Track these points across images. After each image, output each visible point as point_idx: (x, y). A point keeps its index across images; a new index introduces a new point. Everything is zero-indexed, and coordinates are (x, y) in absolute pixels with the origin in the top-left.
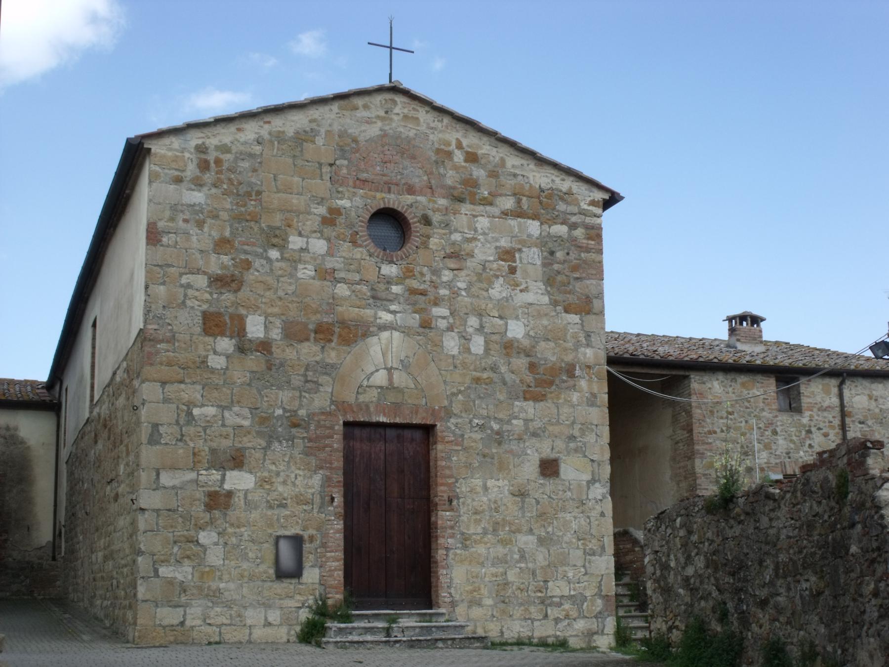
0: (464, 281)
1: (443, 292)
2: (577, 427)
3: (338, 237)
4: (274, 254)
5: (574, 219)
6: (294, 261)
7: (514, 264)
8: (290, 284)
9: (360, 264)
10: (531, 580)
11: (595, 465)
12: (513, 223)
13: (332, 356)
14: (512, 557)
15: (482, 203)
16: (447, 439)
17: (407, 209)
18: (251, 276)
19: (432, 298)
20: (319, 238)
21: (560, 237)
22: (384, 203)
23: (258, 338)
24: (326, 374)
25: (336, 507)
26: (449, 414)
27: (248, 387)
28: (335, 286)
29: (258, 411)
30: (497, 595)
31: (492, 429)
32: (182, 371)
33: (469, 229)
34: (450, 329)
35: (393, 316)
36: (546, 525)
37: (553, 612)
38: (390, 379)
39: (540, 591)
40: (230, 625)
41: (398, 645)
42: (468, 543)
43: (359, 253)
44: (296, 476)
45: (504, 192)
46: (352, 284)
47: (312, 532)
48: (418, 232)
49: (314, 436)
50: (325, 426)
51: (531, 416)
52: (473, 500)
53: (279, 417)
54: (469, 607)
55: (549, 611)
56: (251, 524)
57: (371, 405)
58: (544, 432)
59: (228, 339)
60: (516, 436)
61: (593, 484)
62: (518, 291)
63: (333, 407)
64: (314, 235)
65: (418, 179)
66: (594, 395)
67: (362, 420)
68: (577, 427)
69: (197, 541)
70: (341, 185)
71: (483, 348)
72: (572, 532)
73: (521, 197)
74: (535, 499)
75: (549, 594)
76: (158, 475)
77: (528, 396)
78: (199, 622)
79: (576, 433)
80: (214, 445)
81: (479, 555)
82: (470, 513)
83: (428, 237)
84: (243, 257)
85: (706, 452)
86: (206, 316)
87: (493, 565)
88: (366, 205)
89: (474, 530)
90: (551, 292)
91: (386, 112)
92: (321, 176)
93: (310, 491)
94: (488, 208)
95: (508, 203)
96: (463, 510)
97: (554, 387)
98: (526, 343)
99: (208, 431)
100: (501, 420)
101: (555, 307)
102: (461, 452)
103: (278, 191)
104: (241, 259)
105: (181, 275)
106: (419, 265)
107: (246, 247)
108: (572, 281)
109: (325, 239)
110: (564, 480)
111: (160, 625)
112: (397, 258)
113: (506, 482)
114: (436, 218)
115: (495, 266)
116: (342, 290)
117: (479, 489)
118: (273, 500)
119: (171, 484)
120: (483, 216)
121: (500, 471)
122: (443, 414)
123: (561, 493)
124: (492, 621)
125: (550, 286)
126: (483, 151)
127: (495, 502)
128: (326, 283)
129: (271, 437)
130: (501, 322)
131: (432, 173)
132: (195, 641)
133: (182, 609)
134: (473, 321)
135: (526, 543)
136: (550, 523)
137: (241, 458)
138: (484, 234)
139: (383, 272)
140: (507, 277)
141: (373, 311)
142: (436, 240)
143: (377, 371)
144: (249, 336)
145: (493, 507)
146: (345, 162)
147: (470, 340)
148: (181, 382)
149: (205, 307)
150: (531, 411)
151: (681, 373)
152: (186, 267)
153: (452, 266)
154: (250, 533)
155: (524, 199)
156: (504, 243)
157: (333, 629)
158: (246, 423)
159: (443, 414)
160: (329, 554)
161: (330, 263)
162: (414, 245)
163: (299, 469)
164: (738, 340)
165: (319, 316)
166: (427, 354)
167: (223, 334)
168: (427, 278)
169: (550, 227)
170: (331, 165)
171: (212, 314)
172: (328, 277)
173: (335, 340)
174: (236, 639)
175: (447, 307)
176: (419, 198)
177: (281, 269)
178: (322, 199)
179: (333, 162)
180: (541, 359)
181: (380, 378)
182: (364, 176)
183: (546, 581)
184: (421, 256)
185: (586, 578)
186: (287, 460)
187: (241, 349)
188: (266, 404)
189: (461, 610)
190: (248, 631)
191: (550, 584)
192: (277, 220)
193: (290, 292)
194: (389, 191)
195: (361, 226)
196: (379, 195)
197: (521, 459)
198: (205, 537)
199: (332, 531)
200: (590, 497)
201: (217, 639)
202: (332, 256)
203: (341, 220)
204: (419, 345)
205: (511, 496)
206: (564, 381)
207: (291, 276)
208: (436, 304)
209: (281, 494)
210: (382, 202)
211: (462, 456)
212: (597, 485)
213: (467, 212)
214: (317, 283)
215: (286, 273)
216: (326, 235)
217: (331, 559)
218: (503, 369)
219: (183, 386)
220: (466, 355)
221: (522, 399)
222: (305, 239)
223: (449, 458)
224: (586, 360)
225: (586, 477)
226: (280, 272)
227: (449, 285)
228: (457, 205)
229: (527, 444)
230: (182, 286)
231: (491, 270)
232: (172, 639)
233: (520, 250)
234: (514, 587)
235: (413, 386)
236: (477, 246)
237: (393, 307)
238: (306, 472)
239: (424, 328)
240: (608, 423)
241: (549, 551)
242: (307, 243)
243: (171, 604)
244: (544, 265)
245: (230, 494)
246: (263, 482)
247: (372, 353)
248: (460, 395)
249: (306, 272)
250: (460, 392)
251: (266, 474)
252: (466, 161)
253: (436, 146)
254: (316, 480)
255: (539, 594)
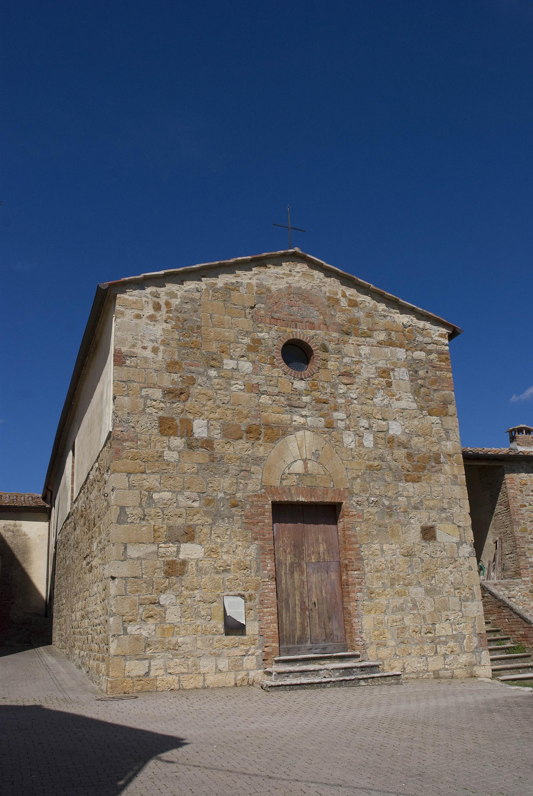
0: (355, 393)
1: (340, 401)
2: (446, 501)
3: (260, 360)
4: (213, 373)
5: (429, 347)
6: (228, 379)
7: (390, 380)
8: (226, 396)
9: (278, 380)
10: (423, 623)
11: (461, 529)
12: (387, 350)
13: (261, 451)
14: (407, 606)
15: (363, 335)
16: (351, 514)
17: (310, 340)
18: (195, 390)
19: (333, 405)
20: (246, 361)
21: (421, 360)
22: (293, 336)
23: (202, 438)
24: (257, 464)
25: (270, 571)
26: (352, 494)
27: (196, 476)
28: (260, 397)
29: (205, 495)
30: (398, 637)
31: (384, 505)
32: (144, 464)
33: (356, 355)
34: (348, 428)
35: (304, 419)
36: (430, 578)
37: (441, 649)
38: (306, 467)
39: (430, 633)
40: (187, 673)
41: (328, 685)
42: (373, 595)
43: (276, 372)
44: (236, 546)
45: (378, 328)
46: (273, 396)
47: (251, 592)
48: (319, 356)
49: (249, 514)
50: (258, 506)
51: (411, 494)
52: (374, 561)
53: (222, 499)
54: (377, 649)
55: (439, 650)
56: (203, 587)
57: (292, 488)
58: (422, 505)
59: (180, 438)
60: (402, 510)
61: (462, 545)
62: (394, 400)
63: (263, 490)
64: (242, 359)
65: (317, 317)
66: (455, 477)
67: (286, 500)
68: (446, 501)
69: (158, 603)
70: (260, 322)
71: (372, 443)
72: (450, 584)
73: (390, 331)
74: (420, 558)
75: (437, 635)
76: (125, 548)
77: (408, 478)
78: (161, 672)
79: (446, 506)
80: (171, 523)
81: (382, 605)
82: (373, 571)
83: (326, 360)
84: (189, 375)
85: (520, 520)
86: (162, 420)
87: (393, 613)
88: (279, 337)
89: (376, 585)
90: (418, 400)
91: (290, 271)
92: (246, 316)
93: (248, 558)
94: (368, 339)
95: (382, 336)
96: (367, 569)
97: (426, 471)
98: (404, 438)
99: (165, 512)
100: (390, 497)
101: (422, 411)
102: (363, 524)
103: (214, 326)
104: (187, 377)
105: (141, 388)
106: (321, 381)
107: (193, 368)
108: (432, 392)
109: (251, 362)
110: (440, 543)
111: (129, 676)
112: (305, 376)
113: (398, 546)
114: (331, 346)
115: (376, 382)
116: (264, 399)
117: (378, 552)
118: (220, 567)
119: (137, 556)
120: (365, 345)
121: (393, 537)
122: (347, 494)
123: (438, 553)
124: (396, 660)
125: (417, 395)
126: (361, 299)
127: (391, 562)
128: (253, 394)
129: (216, 515)
130: (384, 423)
131: (326, 314)
132: (159, 689)
133: (146, 662)
134: (364, 423)
135: (416, 594)
136: (433, 577)
137: (193, 533)
138: (367, 358)
139: (295, 386)
140: (386, 389)
141: (290, 416)
142: (333, 363)
143: (295, 461)
144: (196, 435)
145: (389, 565)
146: (263, 306)
147: (362, 436)
148: (144, 473)
149: (161, 413)
150: (411, 489)
151: (497, 464)
152: (144, 383)
153: (346, 381)
154: (202, 595)
155: (393, 333)
156: (381, 364)
157: (274, 673)
158: (196, 504)
159: (347, 494)
160: (265, 610)
161: (255, 380)
162: (316, 366)
163: (239, 541)
164: (518, 444)
165: (248, 420)
166: (332, 448)
167: (175, 435)
168: (328, 391)
169: (412, 353)
170: (252, 308)
171: (167, 419)
172: (254, 390)
173: (262, 439)
174: (192, 686)
175: (344, 412)
176: (318, 332)
177: (218, 384)
178: (247, 332)
179: (253, 305)
180: (415, 450)
181: (298, 467)
182: (276, 316)
183: (433, 624)
184: (322, 375)
185: (463, 620)
186: (228, 533)
187: (190, 446)
188: (211, 489)
189: (371, 651)
190: (202, 678)
191: (437, 626)
192: (214, 347)
193: (226, 402)
194: (296, 327)
195: (276, 352)
196: (288, 330)
197: (406, 527)
198: (164, 599)
199: (267, 591)
200: (460, 555)
201: (177, 686)
202: (257, 374)
203: (261, 348)
204: (326, 441)
205: (402, 557)
206: (433, 467)
207: (226, 389)
208: (336, 410)
209: (225, 562)
210: (291, 335)
211: (364, 526)
212: (464, 545)
213: (353, 342)
214: (247, 395)
215: (222, 387)
216: (251, 359)
217: (268, 614)
218: (389, 458)
219: (144, 476)
220: (361, 448)
221: (404, 481)
222: (236, 362)
223: (354, 528)
224: (448, 450)
225: (456, 539)
226: (218, 387)
227: (344, 395)
228: (346, 338)
229: (410, 516)
230: (142, 397)
231: (373, 384)
232: (139, 688)
233: (393, 370)
234: (411, 630)
235: (323, 473)
236: (362, 367)
237: (304, 413)
238: (244, 542)
239: (328, 428)
240: (467, 498)
241: (434, 600)
242: (237, 364)
243: (137, 657)
244: (412, 381)
245: (184, 563)
246: (211, 552)
247: (291, 448)
248: (358, 479)
249: (237, 386)
250: (358, 476)
251: (214, 546)
252: (349, 306)
253: (328, 294)
254: (253, 549)
255: (429, 635)
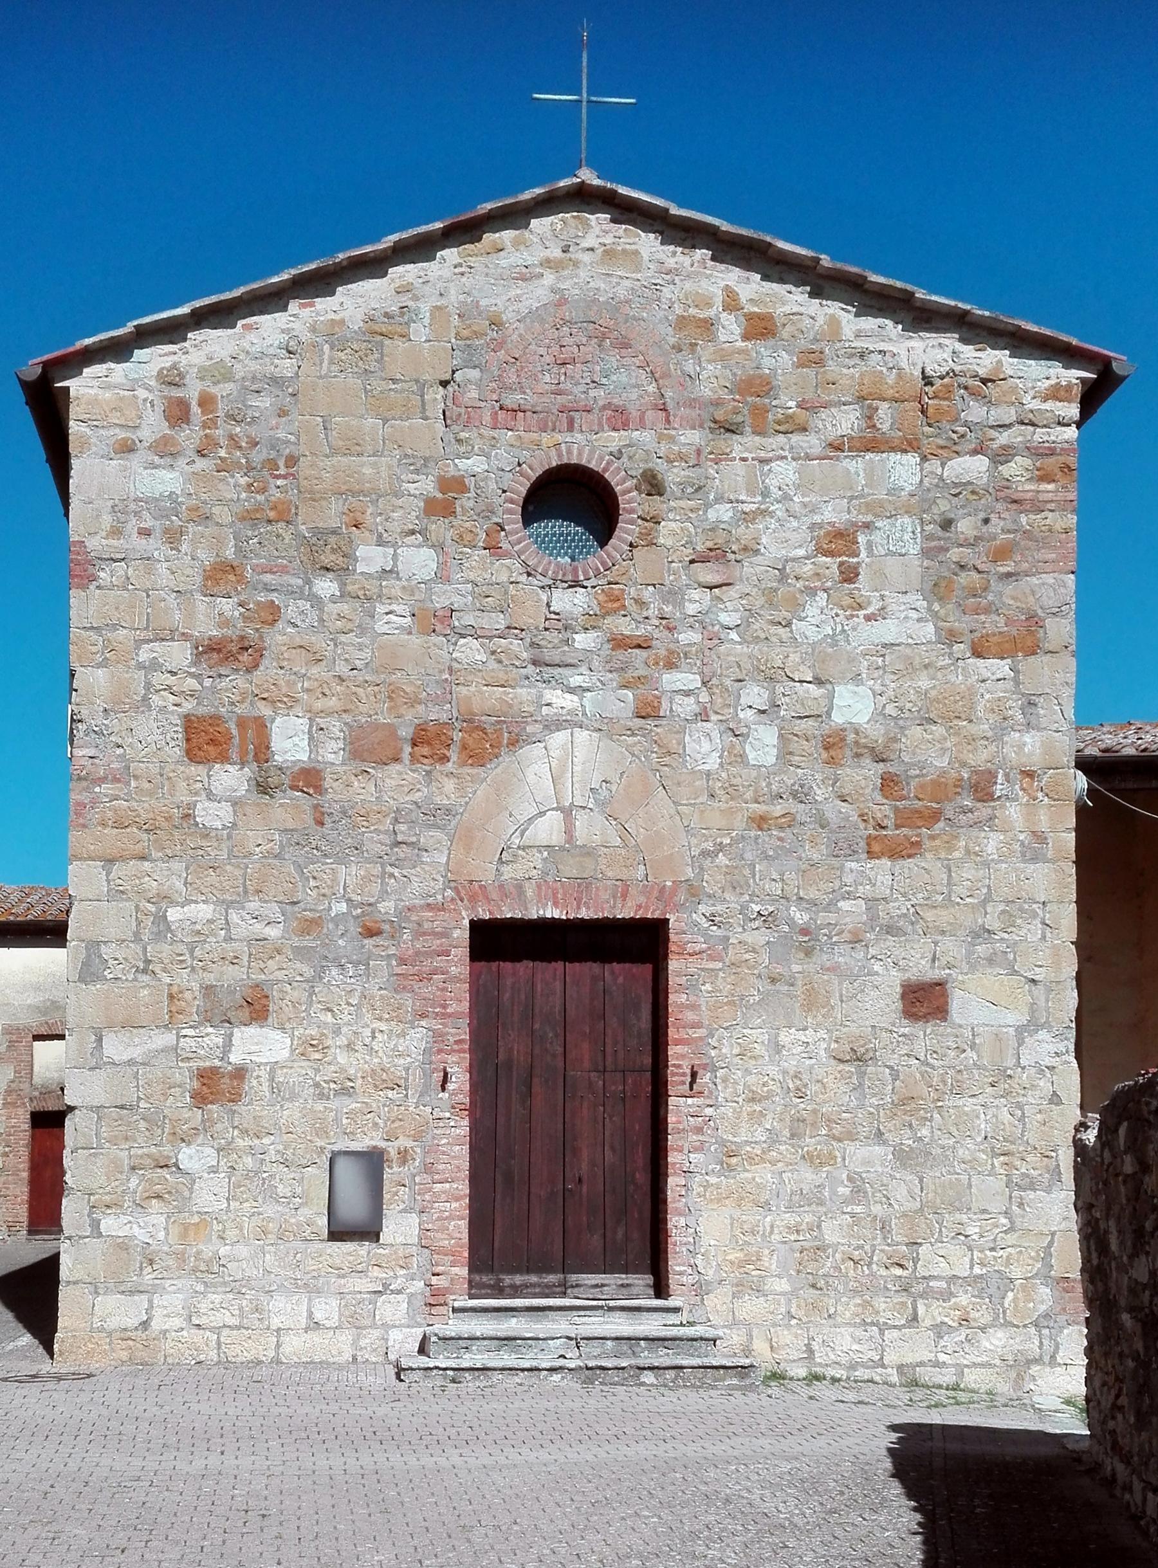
1: (688, 637)
4: (326, 587)
5: (1003, 438)
12: (855, 466)
14: (834, 1192)
16: (690, 948)
18: (277, 638)
19: (663, 652)
20: (419, 546)
21: (970, 483)
22: (560, 455)
24: (435, 826)
25: (453, 1094)
26: (695, 893)
28: (456, 644)
30: (799, 1272)
31: (791, 922)
32: (145, 836)
33: (751, 492)
34: (703, 716)
35: (575, 698)
37: (931, 1312)
38: (569, 832)
40: (238, 1328)
42: (734, 1160)
43: (505, 570)
44: (373, 1032)
46: (490, 638)
47: (404, 1142)
48: (632, 511)
52: (747, 1072)
53: (338, 919)
55: (921, 1310)
57: (527, 884)
59: (237, 767)
60: (846, 936)
63: (449, 893)
66: (1039, 837)
69: (176, 1165)
72: (979, 1139)
75: (922, 1271)
76: (100, 1040)
77: (876, 848)
80: (210, 978)
86: (191, 725)
87: (790, 1208)
90: (942, 612)
93: (402, 1061)
94: (795, 438)
97: (941, 824)
98: (876, 733)
99: (197, 952)
103: (334, 451)
104: (258, 603)
105: (139, 643)
106: (635, 583)
109: (433, 546)
110: (961, 1026)
111: (101, 1329)
112: (585, 573)
113: (822, 1034)
114: (673, 476)
115: (807, 568)
116: (471, 651)
119: (125, 1058)
121: (810, 1010)
122: (682, 897)
126: (787, 309)
127: (797, 1076)
128: (434, 639)
131: (667, 375)
133: (145, 1297)
134: (755, 695)
135: (867, 1162)
137: (264, 1001)
142: (673, 525)
143: (542, 814)
146: (474, 374)
147: (746, 736)
148: (143, 858)
149: (188, 706)
152: (146, 629)
154: (281, 1147)
156: (833, 514)
158: (273, 932)
163: (380, 1019)
165: (421, 708)
167: (224, 758)
168: (652, 612)
169: (943, 465)
170: (444, 384)
171: (201, 719)
174: (249, 1356)
175: (695, 670)
179: (447, 377)
181: (549, 829)
182: (513, 399)
185: (1011, 1239)
187: (263, 788)
189: (717, 1301)
192: (332, 514)
194: (571, 428)
195: (511, 512)
196: (546, 439)
198: (190, 1157)
199: (444, 1141)
200: (1023, 1062)
203: (466, 502)
204: (633, 755)
205: (833, 1062)
206: (966, 811)
207: (362, 630)
208: (671, 665)
209: (343, 1070)
212: (1043, 1034)
214: (416, 640)
215: (350, 626)
218: (820, 793)
219: (147, 865)
222: (391, 551)
224: (1024, 760)
225: (1015, 1018)
227: (700, 621)
230: (141, 666)
232: (124, 1355)
237: (576, 680)
239: (643, 717)
240: (1074, 897)
241: (921, 1181)
242: (395, 556)
243: (122, 1289)
244: (926, 553)
245: (240, 1073)
247: (531, 778)
250: (721, 848)
251: (314, 1032)
252: (746, 337)
253: (678, 310)
254: (417, 1039)
255: (898, 1272)
